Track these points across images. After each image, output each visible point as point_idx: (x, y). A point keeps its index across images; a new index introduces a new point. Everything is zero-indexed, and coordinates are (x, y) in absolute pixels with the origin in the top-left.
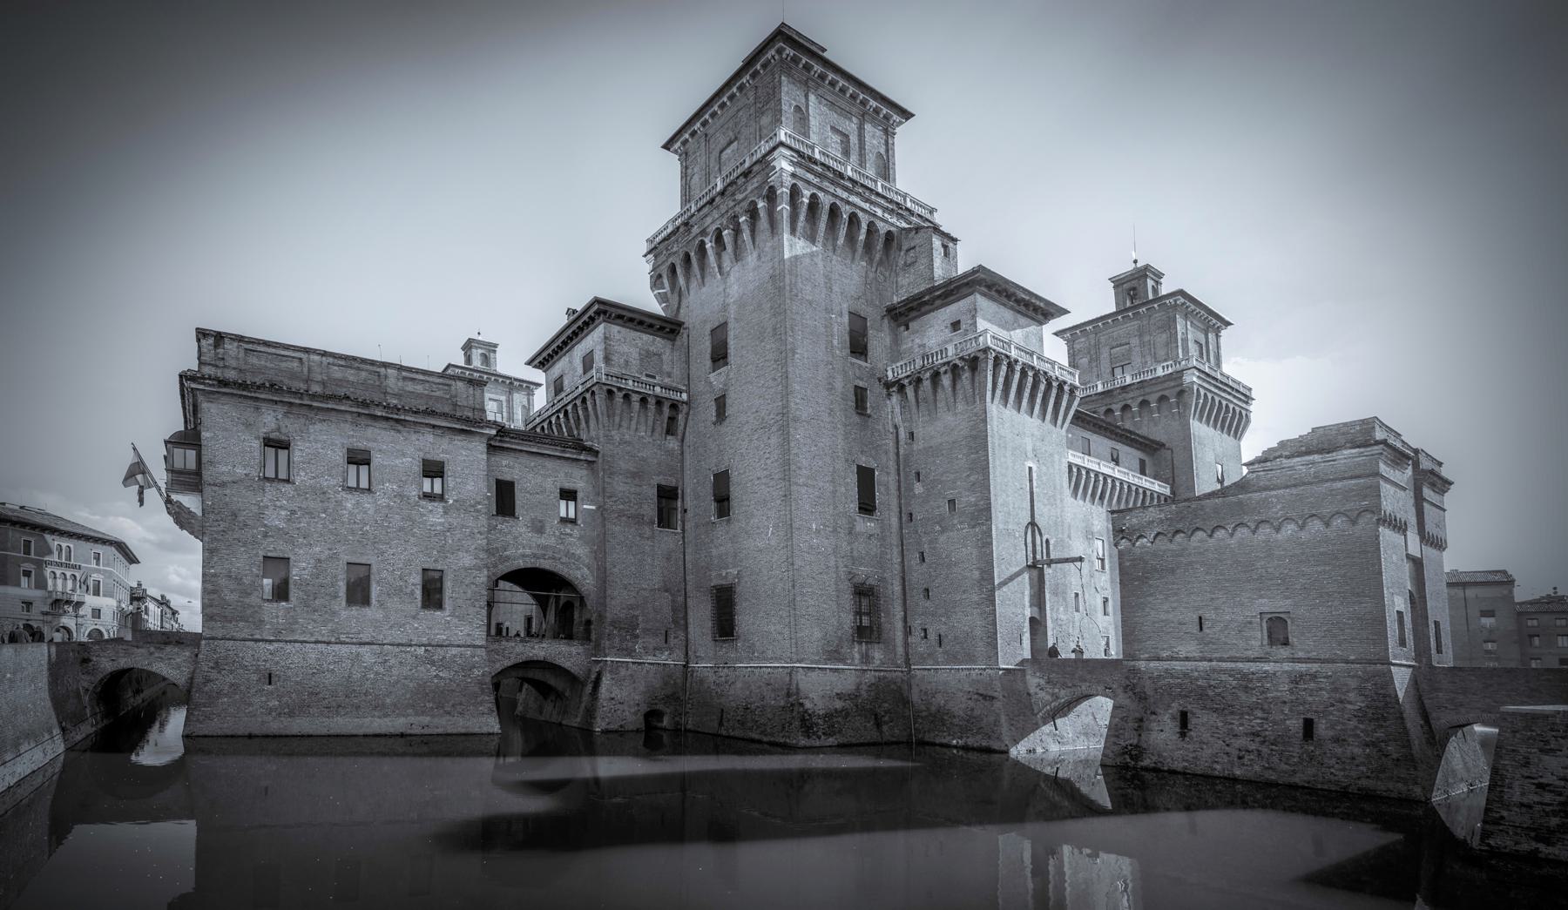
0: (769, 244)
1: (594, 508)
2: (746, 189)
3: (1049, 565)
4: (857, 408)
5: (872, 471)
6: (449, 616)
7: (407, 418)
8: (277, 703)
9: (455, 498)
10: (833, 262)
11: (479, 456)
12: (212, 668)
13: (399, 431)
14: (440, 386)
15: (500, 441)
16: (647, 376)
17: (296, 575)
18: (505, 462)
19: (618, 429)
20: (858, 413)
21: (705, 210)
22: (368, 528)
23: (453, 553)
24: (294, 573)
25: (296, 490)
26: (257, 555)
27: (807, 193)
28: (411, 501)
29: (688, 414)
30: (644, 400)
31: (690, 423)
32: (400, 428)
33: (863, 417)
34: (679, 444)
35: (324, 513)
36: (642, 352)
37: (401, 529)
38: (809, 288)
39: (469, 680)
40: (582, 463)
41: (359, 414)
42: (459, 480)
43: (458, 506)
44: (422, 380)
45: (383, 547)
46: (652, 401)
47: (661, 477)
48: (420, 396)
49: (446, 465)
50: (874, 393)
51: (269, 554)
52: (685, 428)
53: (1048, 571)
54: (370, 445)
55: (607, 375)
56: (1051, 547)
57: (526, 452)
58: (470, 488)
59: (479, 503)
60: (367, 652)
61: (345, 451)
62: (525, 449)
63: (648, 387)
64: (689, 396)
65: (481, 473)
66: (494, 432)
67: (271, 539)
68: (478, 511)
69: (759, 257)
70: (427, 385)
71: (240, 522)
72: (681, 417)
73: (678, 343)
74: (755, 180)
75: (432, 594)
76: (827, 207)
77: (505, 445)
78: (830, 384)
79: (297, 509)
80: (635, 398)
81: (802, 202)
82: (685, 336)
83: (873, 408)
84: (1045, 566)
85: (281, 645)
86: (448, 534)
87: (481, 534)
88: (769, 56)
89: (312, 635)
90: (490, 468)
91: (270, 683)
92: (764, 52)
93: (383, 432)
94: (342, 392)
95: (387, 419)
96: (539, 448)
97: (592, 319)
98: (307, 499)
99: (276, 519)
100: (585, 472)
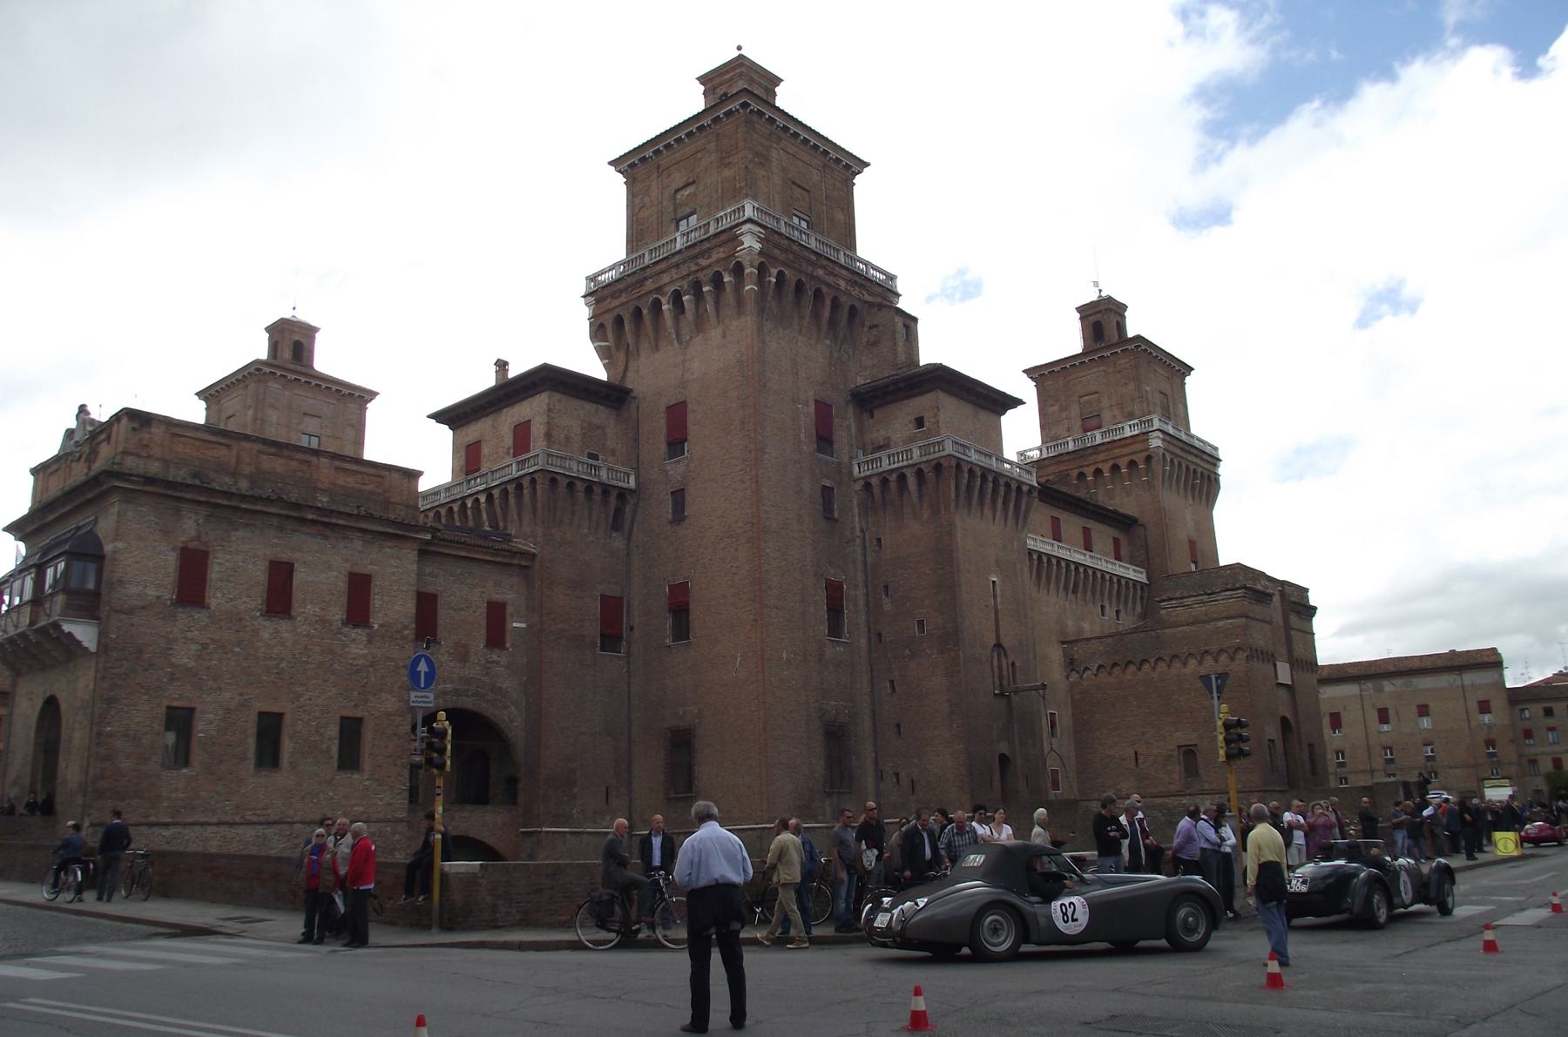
0: (735, 323)
3: (1015, 693)
4: (824, 510)
6: (367, 780)
9: (381, 622)
10: (799, 344)
17: (201, 731)
20: (826, 518)
23: (374, 695)
24: (199, 728)
27: (774, 271)
29: (636, 505)
35: (238, 646)
45: (299, 689)
46: (597, 490)
51: (175, 704)
53: (1015, 699)
56: (1018, 672)
59: (406, 627)
69: (724, 336)
72: (628, 509)
74: (721, 250)
76: (793, 285)
79: (208, 641)
80: (580, 486)
81: (770, 281)
84: (1012, 694)
86: (371, 669)
90: (420, 574)
98: (221, 627)
99: (184, 657)
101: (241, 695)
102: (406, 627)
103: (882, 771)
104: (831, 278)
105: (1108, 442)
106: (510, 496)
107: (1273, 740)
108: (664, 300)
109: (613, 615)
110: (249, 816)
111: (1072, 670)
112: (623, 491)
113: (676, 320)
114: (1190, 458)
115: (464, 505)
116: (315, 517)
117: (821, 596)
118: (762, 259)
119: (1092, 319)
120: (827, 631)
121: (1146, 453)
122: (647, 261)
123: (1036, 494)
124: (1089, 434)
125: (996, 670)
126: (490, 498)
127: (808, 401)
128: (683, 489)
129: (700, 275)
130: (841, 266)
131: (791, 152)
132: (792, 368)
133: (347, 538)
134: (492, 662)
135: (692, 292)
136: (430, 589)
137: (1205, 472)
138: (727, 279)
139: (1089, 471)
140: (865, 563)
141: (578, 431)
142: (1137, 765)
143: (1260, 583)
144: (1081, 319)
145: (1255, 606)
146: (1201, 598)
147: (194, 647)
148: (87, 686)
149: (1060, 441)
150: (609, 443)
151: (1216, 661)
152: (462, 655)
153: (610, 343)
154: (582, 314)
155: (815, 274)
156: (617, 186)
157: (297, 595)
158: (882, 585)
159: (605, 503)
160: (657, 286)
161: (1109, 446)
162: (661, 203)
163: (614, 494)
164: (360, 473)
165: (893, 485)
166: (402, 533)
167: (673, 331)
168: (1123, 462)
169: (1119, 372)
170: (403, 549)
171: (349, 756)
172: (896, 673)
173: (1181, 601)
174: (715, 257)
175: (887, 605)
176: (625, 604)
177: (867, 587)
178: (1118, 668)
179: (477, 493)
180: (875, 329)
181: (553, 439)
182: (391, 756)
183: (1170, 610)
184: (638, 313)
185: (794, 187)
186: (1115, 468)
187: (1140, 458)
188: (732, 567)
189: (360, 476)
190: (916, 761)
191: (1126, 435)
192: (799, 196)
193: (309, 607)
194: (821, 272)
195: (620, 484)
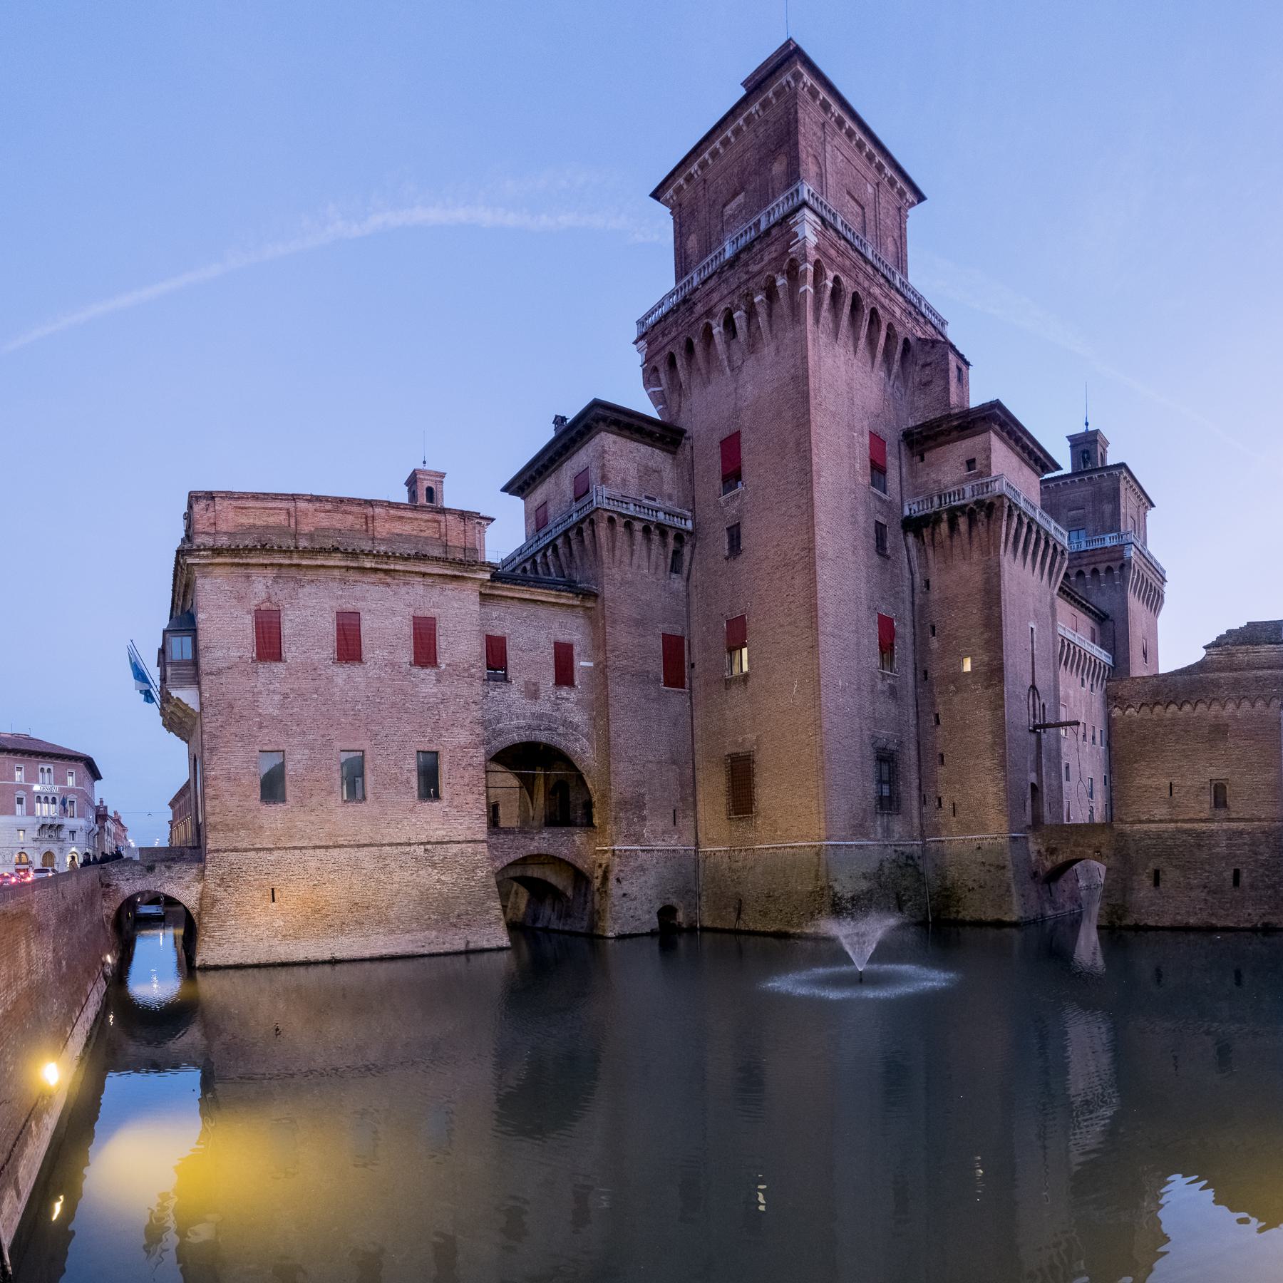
1: (591, 664)
4: (877, 546)
5: (891, 620)
7: (398, 567)
8: (282, 923)
11: (471, 607)
12: (219, 885)
13: (388, 585)
15: (491, 587)
16: (647, 497)
18: (495, 614)
19: (619, 567)
21: (712, 283)
22: (359, 706)
25: (287, 669)
28: (402, 670)
30: (646, 530)
31: (697, 557)
32: (389, 580)
33: (883, 559)
34: (685, 584)
36: (640, 468)
37: (393, 705)
39: (474, 884)
40: (577, 610)
41: (348, 568)
42: (451, 639)
43: (451, 671)
44: (410, 518)
47: (666, 626)
48: (408, 539)
50: (894, 536)
52: (691, 564)
54: (359, 605)
55: (608, 499)
57: (520, 599)
58: (462, 648)
59: (472, 666)
60: (366, 856)
61: (334, 615)
62: (517, 596)
63: (650, 512)
64: (694, 524)
65: (474, 628)
66: (488, 576)
67: (267, 731)
68: (471, 676)
70: (416, 523)
71: (235, 714)
73: (680, 457)
75: (430, 783)
77: (496, 592)
80: (638, 526)
82: (688, 447)
83: (892, 548)
87: (476, 704)
88: (783, 81)
89: (310, 839)
90: (484, 620)
91: (274, 901)
92: (777, 74)
93: (372, 588)
94: (329, 543)
95: (375, 570)
96: (532, 593)
97: (588, 428)
99: (269, 706)
100: (581, 621)
102: (472, 666)
109: (674, 651)
110: (341, 841)
112: (680, 532)
117: (874, 629)
128: (739, 524)
130: (898, 290)
136: (498, 632)
141: (633, 472)
142: (1171, 795)
157: (365, 641)
163: (671, 534)
171: (430, 783)
181: (610, 482)
182: (468, 785)
190: (957, 787)
193: (378, 652)
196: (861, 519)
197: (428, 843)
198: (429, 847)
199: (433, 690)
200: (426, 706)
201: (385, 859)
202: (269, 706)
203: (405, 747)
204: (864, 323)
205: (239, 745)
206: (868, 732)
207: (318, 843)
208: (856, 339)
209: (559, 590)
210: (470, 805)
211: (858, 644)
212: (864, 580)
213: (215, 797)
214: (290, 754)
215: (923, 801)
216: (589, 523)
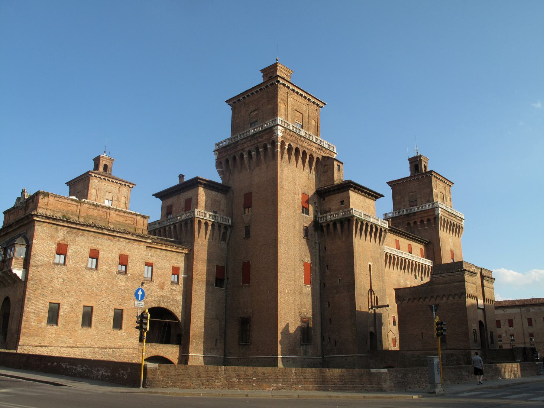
2: (263, 138)
3: (377, 309)
6: (124, 333)
10: (296, 172)
11: (143, 252)
14: (130, 218)
23: (128, 301)
26: (46, 302)
27: (287, 144)
37: (107, 289)
38: (287, 184)
49: (129, 257)
51: (53, 301)
58: (137, 268)
59: (140, 275)
60: (88, 352)
65: (143, 261)
67: (54, 294)
69: (267, 168)
72: (228, 233)
74: (267, 135)
75: (118, 322)
78: (294, 226)
79: (66, 278)
85: (52, 348)
101: (77, 299)
103: (324, 337)
104: (310, 147)
105: (419, 211)
106: (183, 226)
107: (475, 330)
108: (244, 154)
110: (78, 344)
111: (398, 300)
113: (249, 161)
114: (452, 218)
115: (165, 229)
116: (108, 233)
118: (282, 139)
119: (414, 163)
120: (303, 282)
121: (434, 216)
122: (239, 138)
123: (388, 231)
124: (412, 208)
125: (370, 299)
126: (175, 227)
127: (299, 194)
129: (259, 145)
131: (295, 99)
132: (293, 181)
133: (119, 241)
134: (174, 290)
135: (255, 151)
137: (458, 224)
138: (269, 146)
139: (412, 222)
140: (320, 256)
142: (422, 338)
143: (472, 268)
144: (410, 163)
145: (469, 278)
146: (448, 274)
147: (61, 280)
148: (20, 294)
149: (400, 210)
150: (221, 207)
151: (454, 298)
152: (162, 286)
153: (224, 169)
154: (213, 158)
155: (303, 145)
156: (228, 109)
158: (326, 265)
159: (220, 230)
160: (242, 148)
161: (420, 213)
162: (245, 117)
164: (126, 216)
165: (331, 227)
166: (140, 240)
167: (247, 165)
168: (425, 219)
169: (424, 184)
170: (141, 246)
172: (331, 299)
173: (440, 275)
174: (264, 138)
175: (328, 273)
176: (226, 269)
177: (320, 265)
178: (416, 300)
179: (170, 225)
180: (326, 166)
183: (436, 278)
184: (234, 158)
185: (296, 112)
186: (422, 221)
187: (431, 218)
188: (267, 256)
189: (125, 218)
191: (426, 209)
192: (298, 115)
193: (104, 267)
194: (305, 144)
195: (225, 223)
196: (297, 226)
197: (115, 348)
198: (115, 350)
199: (124, 284)
200: (120, 290)
201: (96, 354)
202: (57, 284)
203: (110, 307)
204: (300, 156)
205: (42, 299)
206: (298, 310)
207: (69, 345)
208: (297, 162)
209: (177, 247)
210: (133, 333)
211: (295, 275)
212: (298, 250)
213: (27, 321)
214: (62, 305)
215: (323, 339)
216: (191, 221)
